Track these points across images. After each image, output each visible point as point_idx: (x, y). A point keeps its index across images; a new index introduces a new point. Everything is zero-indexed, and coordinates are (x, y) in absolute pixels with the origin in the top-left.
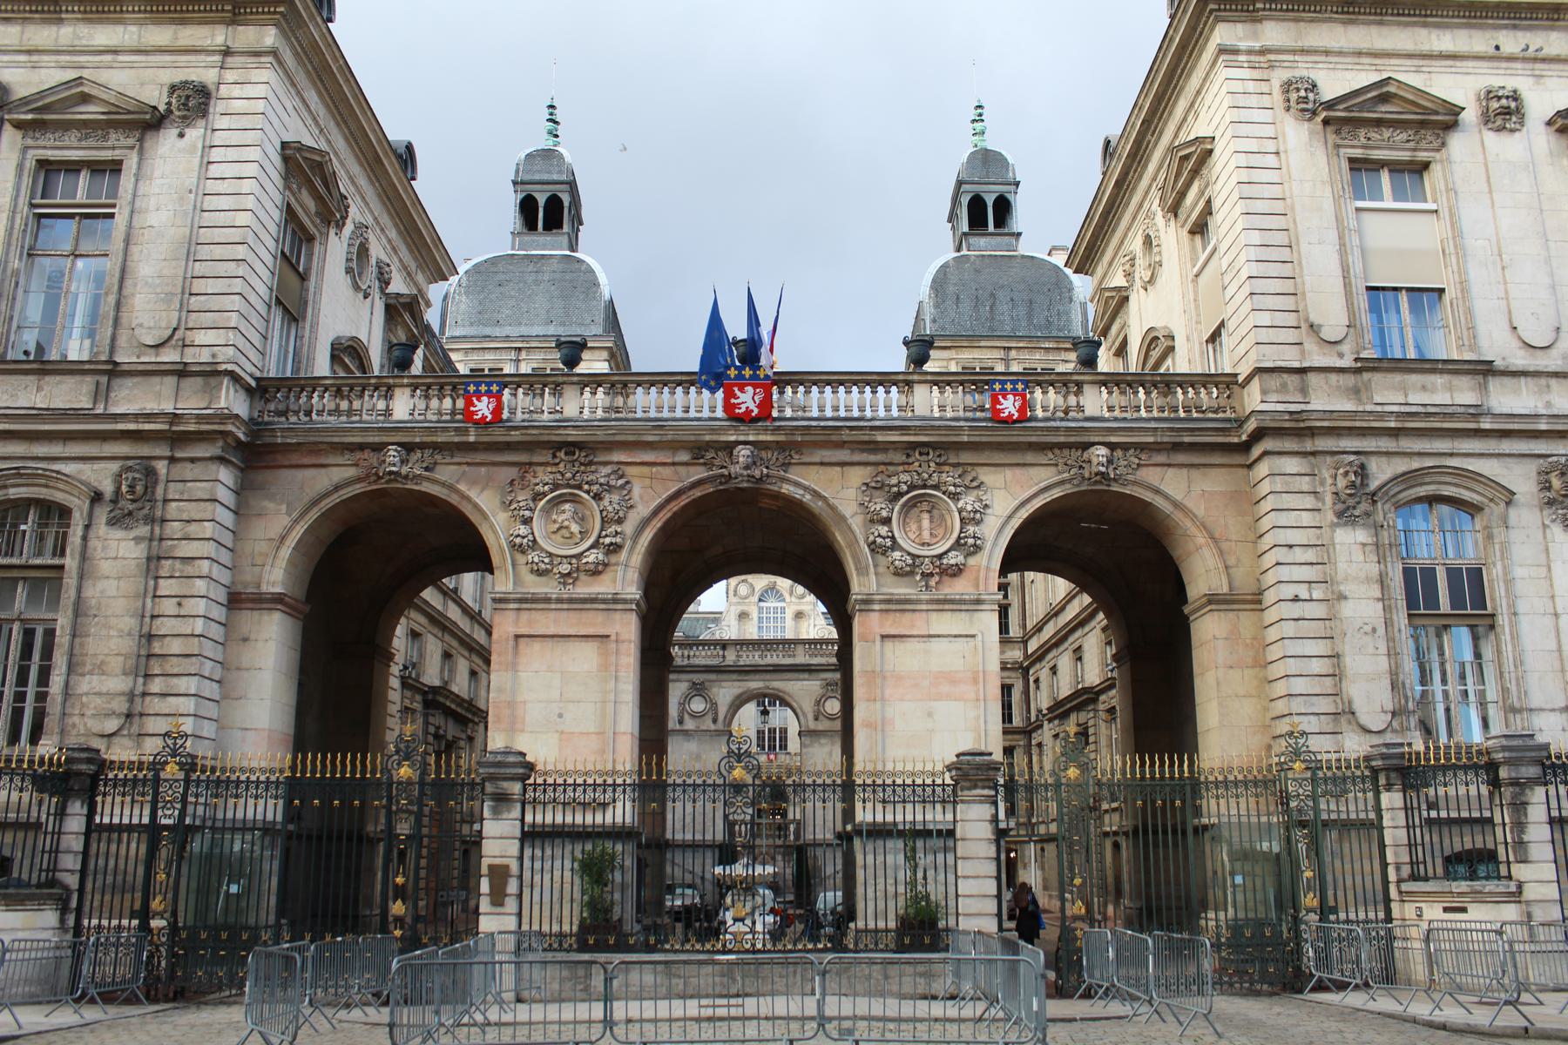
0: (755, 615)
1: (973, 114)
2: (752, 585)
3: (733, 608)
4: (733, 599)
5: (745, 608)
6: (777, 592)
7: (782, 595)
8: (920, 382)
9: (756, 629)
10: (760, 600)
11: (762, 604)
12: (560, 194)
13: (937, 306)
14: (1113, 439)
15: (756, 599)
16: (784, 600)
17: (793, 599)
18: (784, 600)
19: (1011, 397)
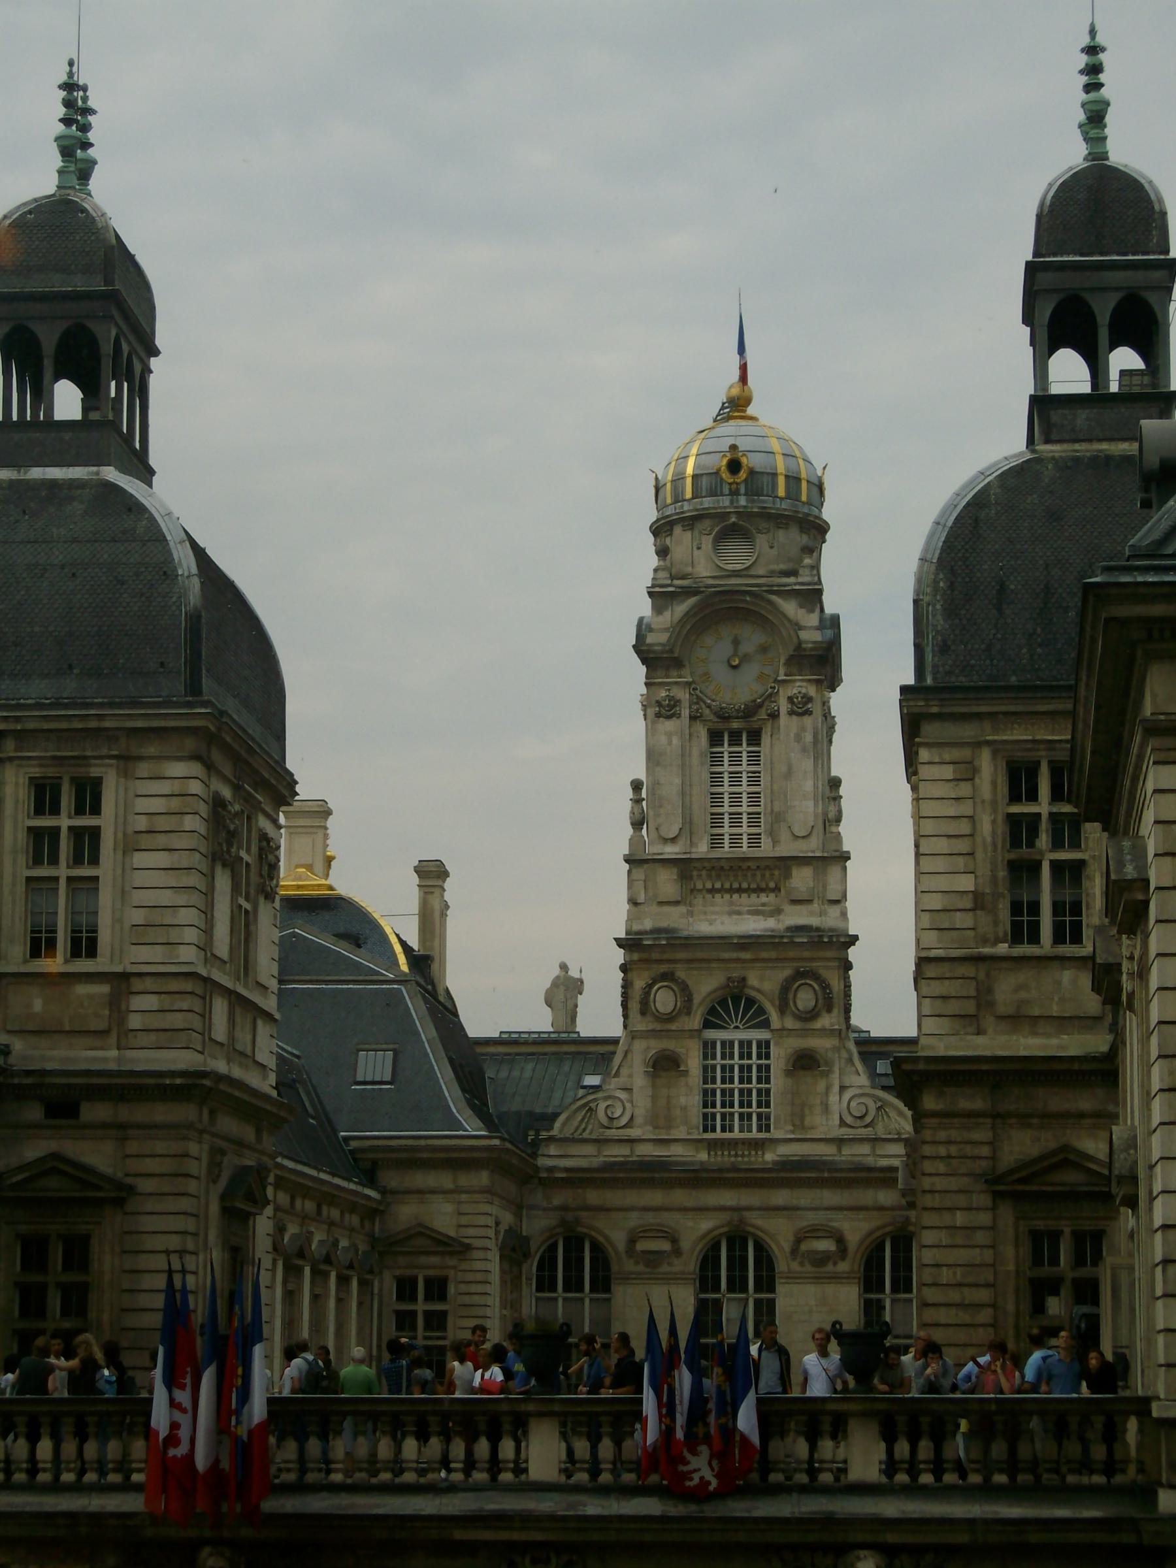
0: (694, 1063)
1: (1083, 60)
2: (685, 992)
3: (639, 1045)
4: (640, 1024)
5: (669, 1045)
6: (751, 1002)
7: (761, 1011)
8: (541, 1415)
9: (696, 1100)
10: (707, 1025)
11: (711, 1034)
12: (92, 326)
13: (950, 611)
14: (891, 1538)
15: (695, 1022)
16: (765, 1024)
17: (790, 1023)
18: (765, 1024)
19: (704, 1449)
